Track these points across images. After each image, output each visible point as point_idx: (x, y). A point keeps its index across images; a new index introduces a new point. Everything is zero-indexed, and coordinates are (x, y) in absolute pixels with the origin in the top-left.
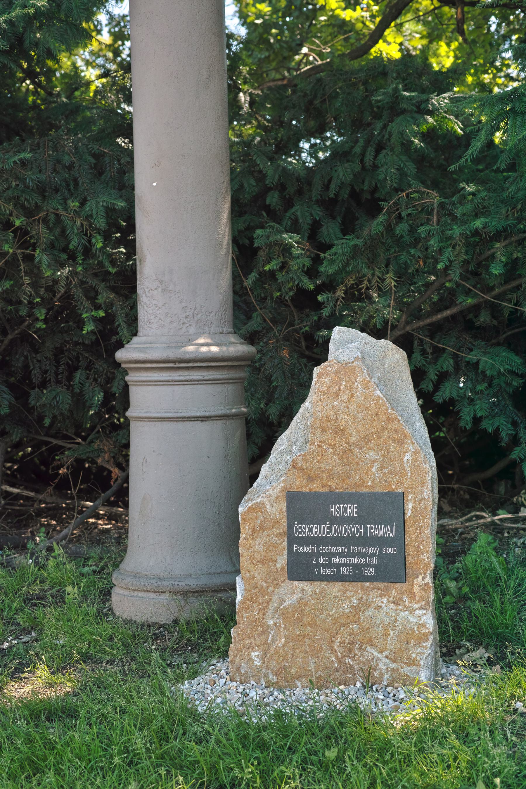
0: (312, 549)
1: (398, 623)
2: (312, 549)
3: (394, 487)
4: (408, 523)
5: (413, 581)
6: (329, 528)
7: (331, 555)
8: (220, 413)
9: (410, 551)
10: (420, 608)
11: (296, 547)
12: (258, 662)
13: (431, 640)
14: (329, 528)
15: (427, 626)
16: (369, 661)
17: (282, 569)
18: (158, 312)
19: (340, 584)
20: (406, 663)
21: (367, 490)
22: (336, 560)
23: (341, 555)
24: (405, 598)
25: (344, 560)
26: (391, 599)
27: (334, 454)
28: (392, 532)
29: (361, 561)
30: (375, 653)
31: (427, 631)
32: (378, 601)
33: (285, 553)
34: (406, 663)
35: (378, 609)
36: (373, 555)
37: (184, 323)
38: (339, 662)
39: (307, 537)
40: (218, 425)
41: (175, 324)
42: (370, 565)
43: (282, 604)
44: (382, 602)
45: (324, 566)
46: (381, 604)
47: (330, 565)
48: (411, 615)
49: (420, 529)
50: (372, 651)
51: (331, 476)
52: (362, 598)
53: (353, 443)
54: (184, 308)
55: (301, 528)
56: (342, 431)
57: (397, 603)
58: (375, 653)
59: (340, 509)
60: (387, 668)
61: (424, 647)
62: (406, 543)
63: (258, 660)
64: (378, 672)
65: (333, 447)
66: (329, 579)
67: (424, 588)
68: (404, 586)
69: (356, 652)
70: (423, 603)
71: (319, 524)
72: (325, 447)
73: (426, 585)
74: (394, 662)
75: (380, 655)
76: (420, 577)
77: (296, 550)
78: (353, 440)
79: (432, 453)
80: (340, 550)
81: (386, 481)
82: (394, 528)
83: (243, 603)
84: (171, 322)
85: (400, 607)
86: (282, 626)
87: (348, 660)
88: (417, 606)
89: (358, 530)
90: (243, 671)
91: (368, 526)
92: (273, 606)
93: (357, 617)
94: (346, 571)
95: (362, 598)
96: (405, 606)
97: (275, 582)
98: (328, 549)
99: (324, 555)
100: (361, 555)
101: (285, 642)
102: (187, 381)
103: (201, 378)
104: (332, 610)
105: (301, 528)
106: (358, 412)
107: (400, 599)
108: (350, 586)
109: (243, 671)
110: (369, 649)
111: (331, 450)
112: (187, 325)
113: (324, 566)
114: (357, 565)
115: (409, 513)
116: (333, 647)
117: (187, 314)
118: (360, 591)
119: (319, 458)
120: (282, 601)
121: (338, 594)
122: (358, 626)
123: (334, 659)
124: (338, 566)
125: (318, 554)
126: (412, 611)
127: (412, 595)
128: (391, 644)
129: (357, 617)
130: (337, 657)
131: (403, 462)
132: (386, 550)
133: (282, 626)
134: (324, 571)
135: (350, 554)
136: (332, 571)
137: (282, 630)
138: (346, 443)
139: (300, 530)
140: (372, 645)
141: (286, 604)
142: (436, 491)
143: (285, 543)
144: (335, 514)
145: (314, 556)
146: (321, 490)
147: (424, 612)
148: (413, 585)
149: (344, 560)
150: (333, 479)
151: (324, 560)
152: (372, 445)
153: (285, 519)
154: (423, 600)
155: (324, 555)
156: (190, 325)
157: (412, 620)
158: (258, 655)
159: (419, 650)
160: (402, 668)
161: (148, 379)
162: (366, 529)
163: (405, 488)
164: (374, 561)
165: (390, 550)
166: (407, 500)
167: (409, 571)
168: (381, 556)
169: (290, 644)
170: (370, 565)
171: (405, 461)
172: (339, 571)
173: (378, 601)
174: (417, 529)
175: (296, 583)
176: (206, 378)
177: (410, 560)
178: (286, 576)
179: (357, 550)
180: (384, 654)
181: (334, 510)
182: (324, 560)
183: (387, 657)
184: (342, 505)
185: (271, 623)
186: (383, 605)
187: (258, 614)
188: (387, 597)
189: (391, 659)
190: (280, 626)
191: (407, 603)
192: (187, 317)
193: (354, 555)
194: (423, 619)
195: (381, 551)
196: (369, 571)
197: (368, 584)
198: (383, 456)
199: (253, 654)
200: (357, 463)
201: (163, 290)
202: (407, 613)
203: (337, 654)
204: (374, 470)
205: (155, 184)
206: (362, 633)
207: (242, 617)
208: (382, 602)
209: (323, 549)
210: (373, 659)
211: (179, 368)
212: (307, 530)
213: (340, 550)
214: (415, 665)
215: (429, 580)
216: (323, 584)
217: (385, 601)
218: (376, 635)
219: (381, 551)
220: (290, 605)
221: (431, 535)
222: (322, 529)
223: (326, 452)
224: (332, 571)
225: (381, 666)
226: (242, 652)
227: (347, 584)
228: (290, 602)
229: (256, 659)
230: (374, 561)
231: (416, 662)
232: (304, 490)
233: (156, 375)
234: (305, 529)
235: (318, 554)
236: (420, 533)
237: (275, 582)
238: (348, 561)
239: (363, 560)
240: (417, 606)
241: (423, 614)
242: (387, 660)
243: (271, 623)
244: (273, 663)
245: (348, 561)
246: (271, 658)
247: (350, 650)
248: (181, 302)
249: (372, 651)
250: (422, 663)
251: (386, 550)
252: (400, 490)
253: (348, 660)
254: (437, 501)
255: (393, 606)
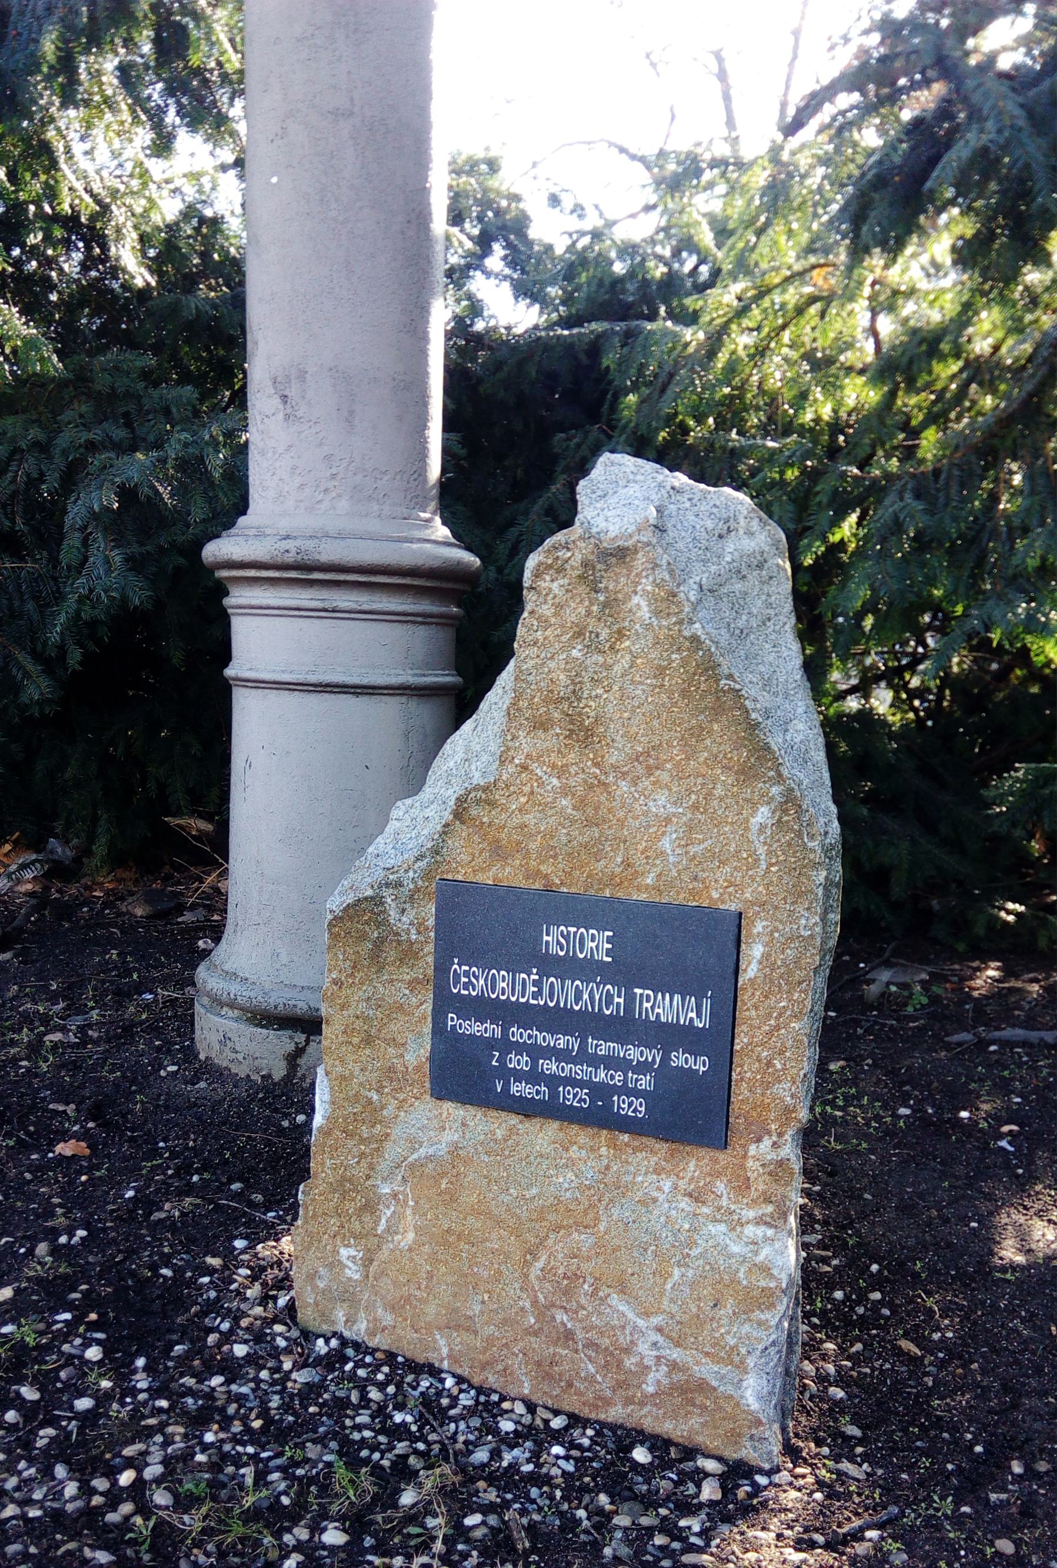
0: (489, 1029)
1: (695, 1252)
2: (489, 1029)
3: (715, 895)
4: (744, 997)
5: (744, 1147)
6: (535, 983)
7: (536, 1052)
8: (393, 681)
9: (745, 1070)
10: (760, 1221)
11: (452, 1020)
12: (353, 1273)
13: (781, 1308)
14: (535, 983)
15: (775, 1272)
16: (613, 1328)
17: (418, 1069)
18: (277, 465)
19: (556, 1125)
20: (707, 1354)
21: (643, 896)
22: (550, 1067)
23: (562, 1055)
24: (720, 1187)
25: (568, 1069)
26: (682, 1184)
27: (565, 791)
28: (699, 1015)
29: (612, 1077)
30: (631, 1315)
31: (772, 1285)
32: (646, 1182)
33: (428, 1029)
34: (707, 1354)
35: (647, 1205)
36: (643, 1068)
37: (326, 490)
38: (540, 1317)
39: (480, 999)
40: (390, 708)
41: (308, 491)
42: (637, 1093)
43: (414, 1150)
44: (659, 1189)
45: (519, 1076)
46: (655, 1194)
47: (534, 1077)
48: (733, 1235)
49: (780, 1015)
50: (622, 1308)
51: (550, 853)
52: (607, 1168)
53: (615, 767)
54: (328, 458)
55: (467, 974)
56: (589, 733)
57: (697, 1197)
58: (631, 1315)
59: (566, 937)
60: (658, 1358)
61: (760, 1323)
62: (737, 1047)
63: (355, 1268)
64: (633, 1360)
65: (561, 771)
66: (526, 1109)
67: (778, 1170)
68: (723, 1157)
69: (583, 1301)
70: (770, 1209)
71: (513, 971)
72: (538, 771)
73: (780, 1163)
74: (678, 1345)
75: (641, 1323)
76: (767, 1142)
77: (453, 1027)
78: (613, 757)
79: (834, 809)
80: (562, 1042)
81: (695, 878)
82: (707, 1004)
83: (326, 1132)
84: (302, 486)
85: (705, 1210)
86: (411, 1203)
87: (561, 1316)
88: (751, 1214)
89: (609, 998)
90: (321, 1285)
91: (638, 991)
92: (393, 1151)
93: (591, 1215)
94: (574, 1097)
95: (607, 1168)
96: (719, 1209)
97: (401, 1096)
98: (530, 1037)
99: (520, 1048)
100: (610, 1062)
101: (415, 1242)
102: (325, 610)
103: (353, 606)
104: (530, 1186)
105: (467, 974)
106: (633, 682)
107: (709, 1189)
108: (583, 1136)
109: (321, 1285)
110: (615, 1300)
111: (555, 781)
112: (334, 494)
113: (519, 1076)
114: (602, 1085)
115: (750, 970)
116: (526, 1276)
117: (334, 471)
118: (603, 1150)
119: (523, 800)
120: (414, 1143)
121: (548, 1149)
122: (591, 1240)
123: (528, 1305)
124: (553, 1082)
125: (506, 1046)
126: (736, 1225)
127: (742, 1185)
128: (672, 1301)
129: (591, 1215)
130: (535, 1302)
131: (747, 829)
132: (680, 1059)
133: (411, 1203)
134: (517, 1088)
135: (584, 1057)
136: (538, 1092)
137: (409, 1212)
138: (596, 765)
139: (464, 980)
140: (623, 1290)
141: (422, 1152)
142: (835, 917)
143: (428, 1007)
144: (554, 949)
145: (493, 1048)
146: (520, 882)
147: (770, 1232)
148: (745, 1156)
149: (568, 1069)
150: (555, 857)
151: (519, 1062)
152: (665, 777)
153: (430, 948)
154: (768, 1201)
155: (520, 1048)
156: (339, 496)
157: (735, 1249)
158: (354, 1257)
159: (746, 1328)
160: (698, 1363)
161: (254, 602)
162: (630, 999)
163: (746, 901)
164: (645, 1082)
165: (691, 1060)
166: (749, 935)
167: (737, 1122)
168: (664, 1072)
169: (426, 1249)
170: (637, 1093)
171: (754, 829)
172: (553, 1095)
173: (646, 1182)
174: (769, 1016)
175: (448, 1106)
176: (365, 607)
177: (741, 1093)
178: (427, 1085)
179: (604, 1048)
180: (656, 1320)
181: (552, 939)
182: (519, 1062)
183: (659, 1330)
184: (573, 929)
185: (386, 1190)
186: (662, 1197)
187: (358, 1163)
188: (673, 1178)
189: (668, 1337)
190: (406, 1202)
191: (724, 1202)
192: (333, 476)
193: (595, 1061)
194: (765, 1252)
195: (666, 1059)
196: (630, 1105)
197: (626, 1137)
198: (695, 807)
199: (344, 1252)
200: (622, 823)
201: (287, 417)
202: (722, 1228)
203: (536, 1296)
204: (666, 844)
205: (274, 180)
206: (601, 1258)
207: (323, 1164)
208: (659, 1189)
209: (517, 1034)
210: (623, 1327)
211: (311, 583)
212: (482, 982)
213: (562, 1042)
214: (731, 1363)
215: (790, 1151)
216: (514, 1120)
217: (667, 1186)
218: (637, 1269)
219: (666, 1059)
220: (429, 1158)
221: (808, 1036)
222: (518, 988)
223: (541, 785)
224: (538, 1092)
225: (643, 1348)
226: (320, 1241)
227: (575, 1128)
228: (431, 1151)
229: (350, 1264)
230: (645, 1082)
231: (737, 1359)
232: (480, 878)
233: (268, 594)
234: (477, 978)
235: (506, 1046)
236: (777, 1028)
237: (401, 1096)
238: (581, 1071)
239: (619, 1077)
240: (751, 1214)
241: (766, 1239)
242: (659, 1338)
243: (386, 1190)
244: (385, 1283)
245: (581, 1071)
246: (383, 1273)
247: (567, 1292)
248: (321, 444)
249: (622, 1308)
250: (751, 1362)
251: (680, 1059)
252: (733, 907)
253: (561, 1316)
254: (833, 943)
255: (685, 1204)
